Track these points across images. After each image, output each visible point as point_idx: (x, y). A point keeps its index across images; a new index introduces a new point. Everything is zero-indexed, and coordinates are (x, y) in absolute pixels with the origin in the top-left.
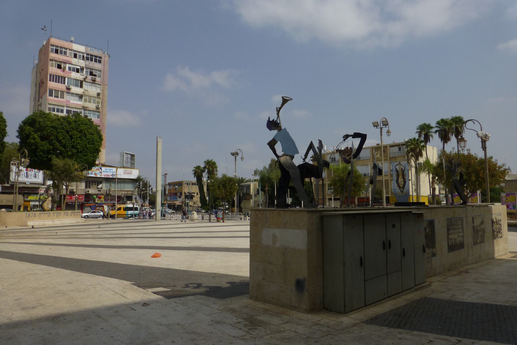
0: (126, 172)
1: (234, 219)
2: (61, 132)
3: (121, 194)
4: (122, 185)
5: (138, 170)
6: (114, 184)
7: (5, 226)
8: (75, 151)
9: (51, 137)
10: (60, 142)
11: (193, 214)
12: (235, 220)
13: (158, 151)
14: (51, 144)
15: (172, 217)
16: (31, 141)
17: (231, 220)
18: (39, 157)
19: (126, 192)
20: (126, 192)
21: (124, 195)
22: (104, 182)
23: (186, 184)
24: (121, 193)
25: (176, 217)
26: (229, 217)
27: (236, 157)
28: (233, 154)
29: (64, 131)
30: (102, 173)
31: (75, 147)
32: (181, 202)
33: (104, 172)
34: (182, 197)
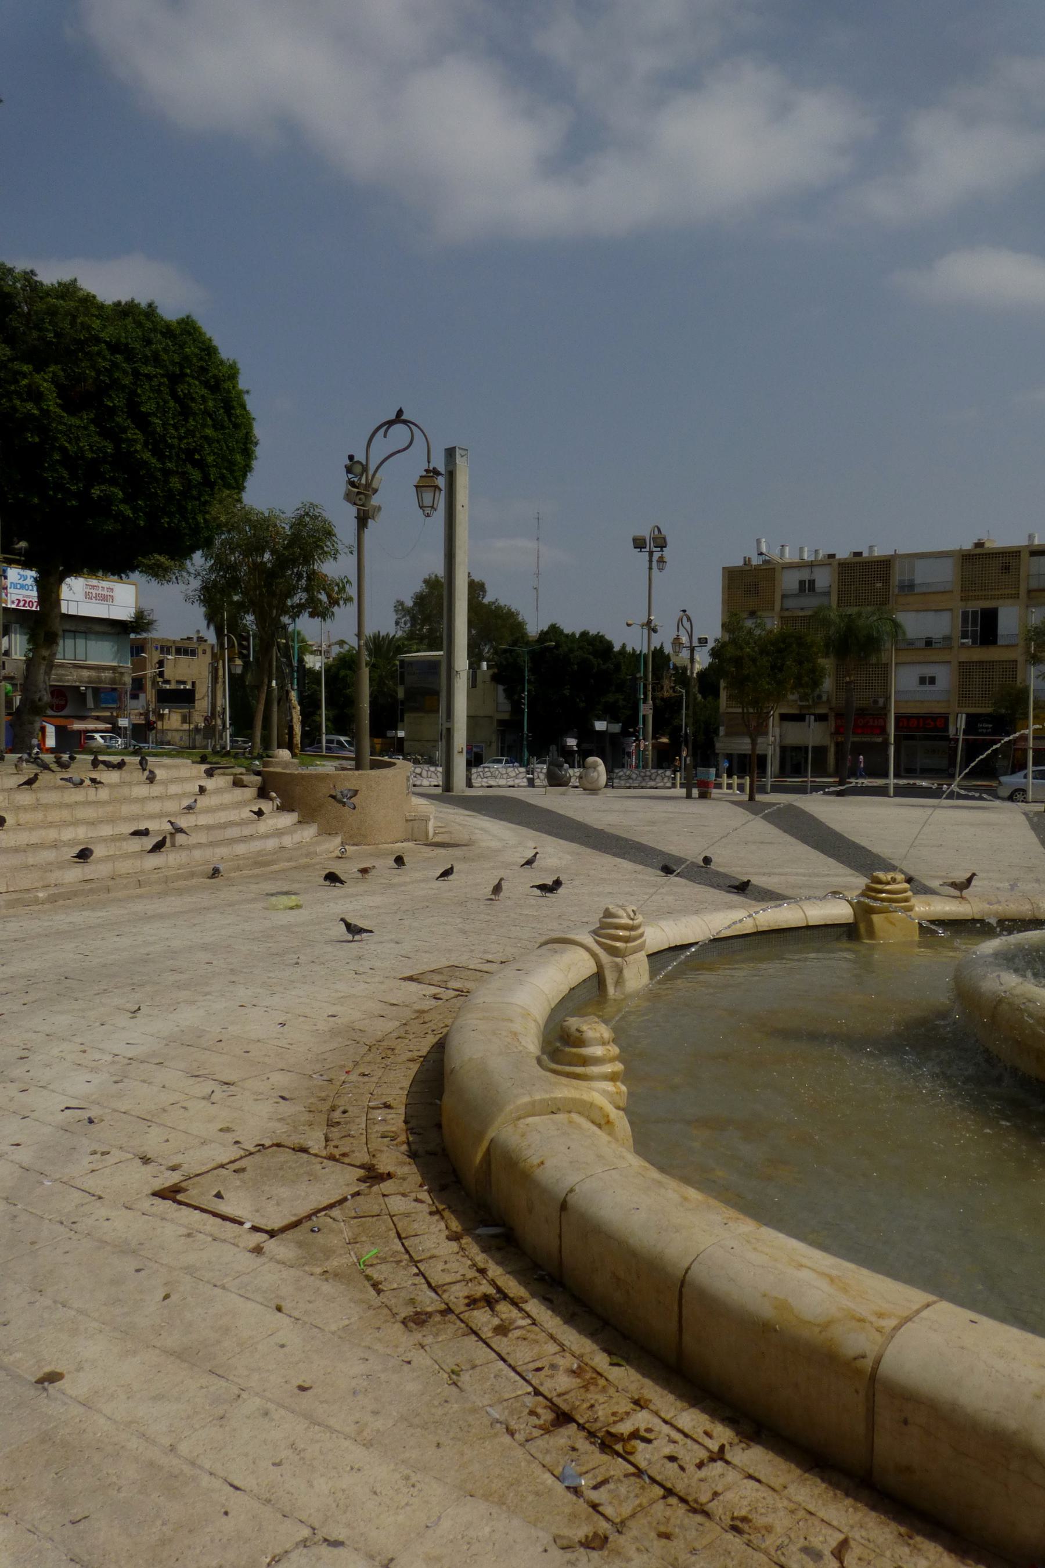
0: (94, 592)
1: (652, 784)
2: (149, 377)
3: (76, 682)
4: (81, 642)
5: (134, 587)
6: (83, 641)
7: (712, 866)
8: (196, 475)
9: (110, 397)
10: (142, 421)
11: (595, 767)
12: (656, 788)
13: (459, 507)
14: (106, 433)
15: (420, 774)
16: (14, 409)
17: (642, 788)
18: (51, 493)
19: (93, 674)
20: (93, 674)
21: (90, 682)
22: (15, 630)
23: (157, 648)
24: (75, 674)
25: (433, 775)
26: (630, 777)
27: (651, 553)
28: (639, 544)
29: (163, 376)
30: (9, 590)
31: (197, 457)
32: (141, 714)
33: (15, 585)
34: (142, 696)
